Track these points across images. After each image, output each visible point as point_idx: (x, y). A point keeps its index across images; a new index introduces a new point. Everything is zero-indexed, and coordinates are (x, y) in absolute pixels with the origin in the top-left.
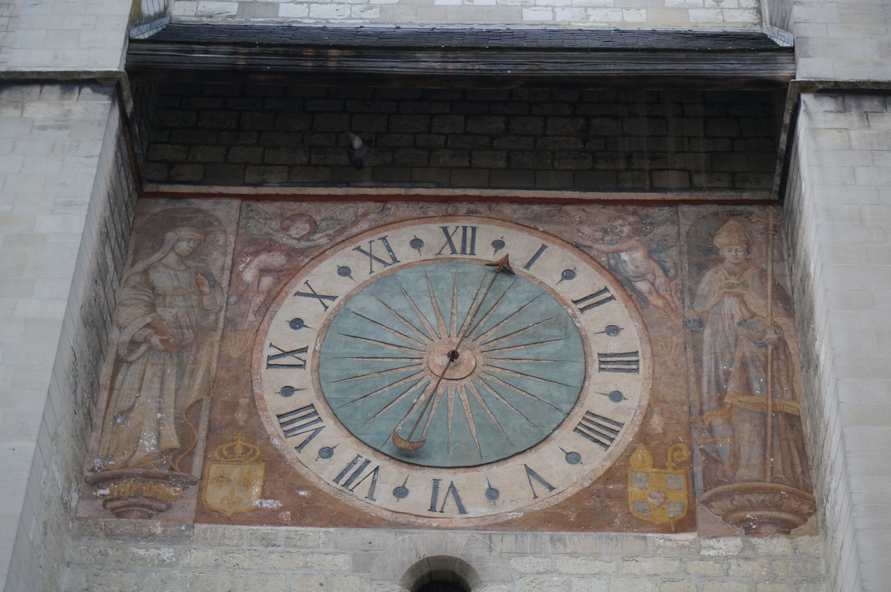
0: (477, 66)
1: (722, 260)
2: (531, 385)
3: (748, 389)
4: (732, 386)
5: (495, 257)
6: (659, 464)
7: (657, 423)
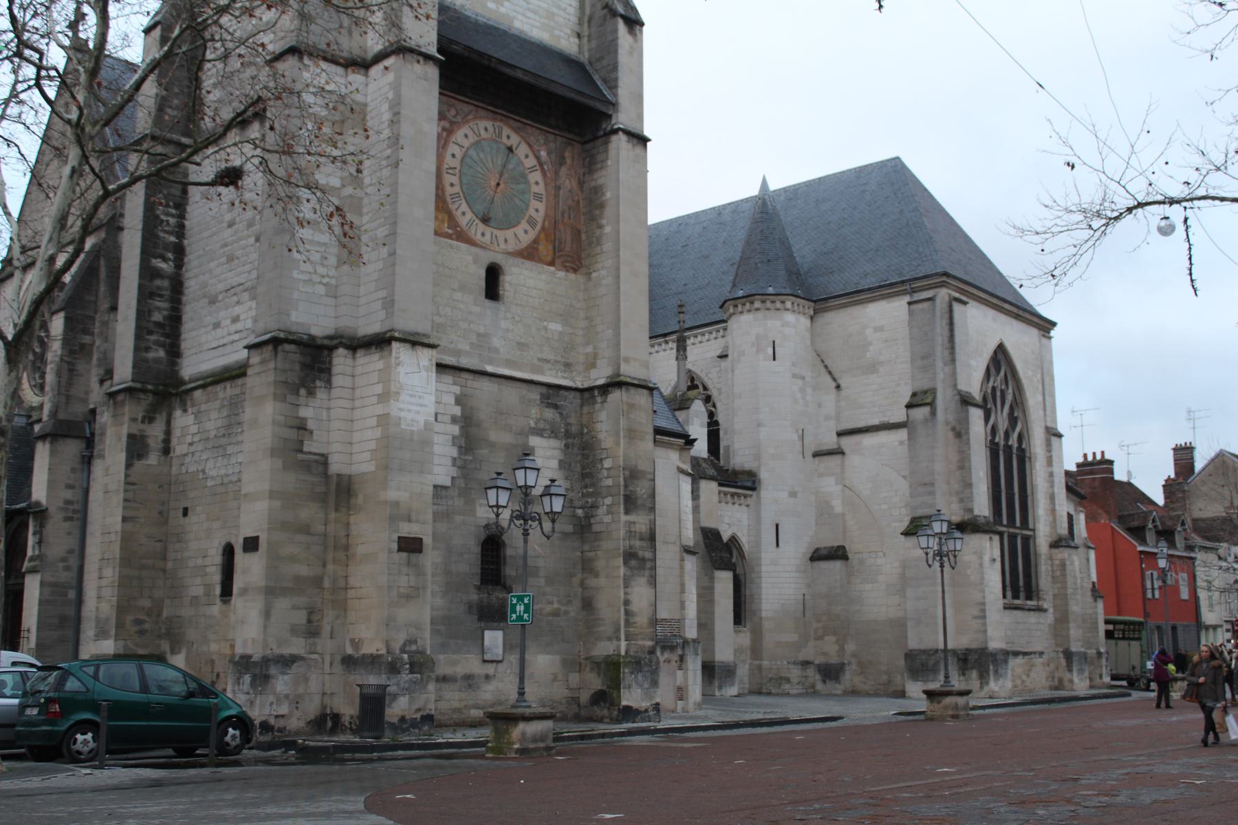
0: (532, 81)
1: (565, 163)
2: (516, 200)
3: (570, 218)
4: (566, 215)
5: (509, 143)
6: (547, 240)
7: (546, 223)
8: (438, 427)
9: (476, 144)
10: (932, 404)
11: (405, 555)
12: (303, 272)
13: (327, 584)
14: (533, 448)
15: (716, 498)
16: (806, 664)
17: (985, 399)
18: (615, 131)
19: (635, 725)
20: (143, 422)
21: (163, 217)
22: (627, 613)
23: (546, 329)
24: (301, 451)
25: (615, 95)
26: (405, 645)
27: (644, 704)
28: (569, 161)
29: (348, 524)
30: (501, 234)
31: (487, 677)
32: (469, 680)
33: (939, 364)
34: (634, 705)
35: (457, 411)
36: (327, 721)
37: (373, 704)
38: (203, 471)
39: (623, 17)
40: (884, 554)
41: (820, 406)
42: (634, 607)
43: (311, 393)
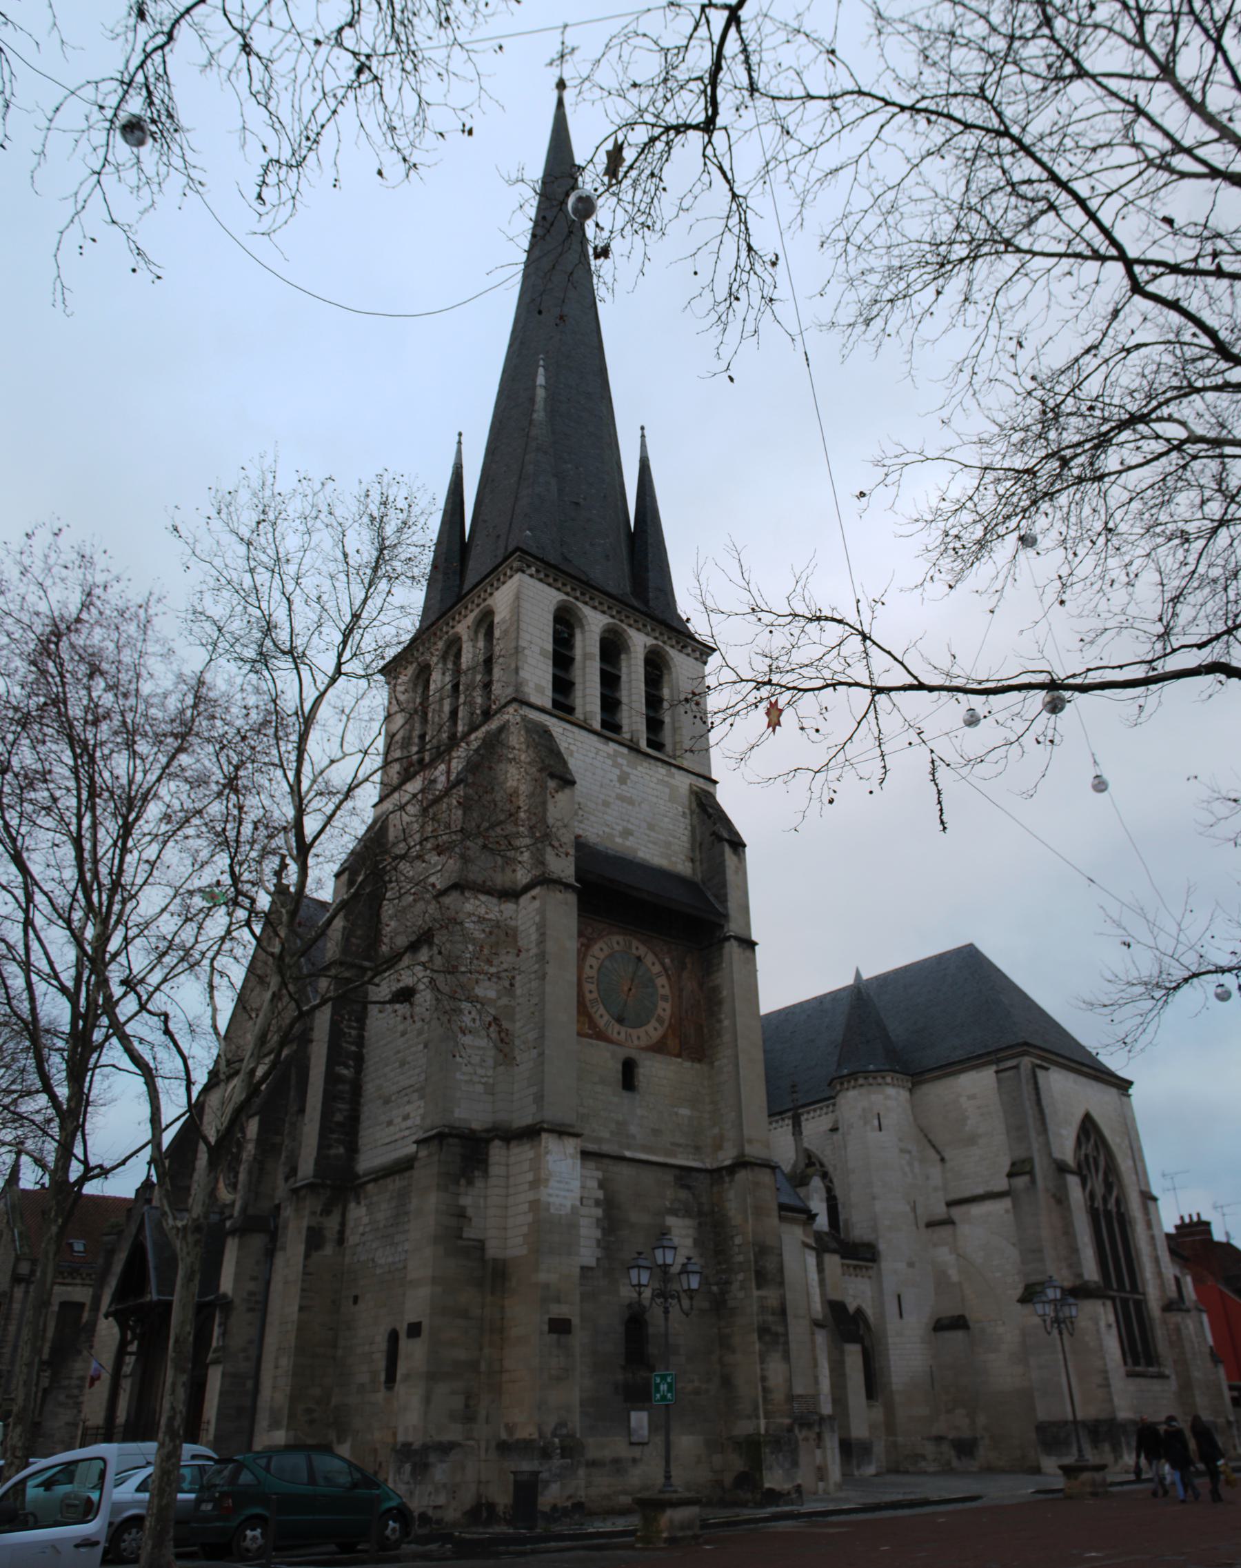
8: (584, 1211)
9: (611, 956)
10: (1031, 1173)
11: (555, 1336)
12: (464, 1074)
13: (483, 1367)
14: (669, 1228)
15: (839, 1271)
16: (939, 1439)
17: (1079, 1165)
18: (728, 938)
19: (779, 1509)
20: (321, 1215)
21: (346, 1030)
22: (766, 1390)
23: (676, 1114)
24: (460, 1238)
25: (726, 908)
26: (556, 1429)
27: (787, 1486)
28: (689, 966)
29: (503, 1307)
30: (634, 1032)
31: (635, 1461)
32: (618, 1465)
33: (1033, 1134)
34: (777, 1487)
35: (600, 1194)
36: (481, 1512)
37: (527, 1489)
38: (373, 1260)
39: (728, 841)
40: (1004, 1323)
41: (928, 1178)
42: (771, 1383)
43: (470, 1183)
